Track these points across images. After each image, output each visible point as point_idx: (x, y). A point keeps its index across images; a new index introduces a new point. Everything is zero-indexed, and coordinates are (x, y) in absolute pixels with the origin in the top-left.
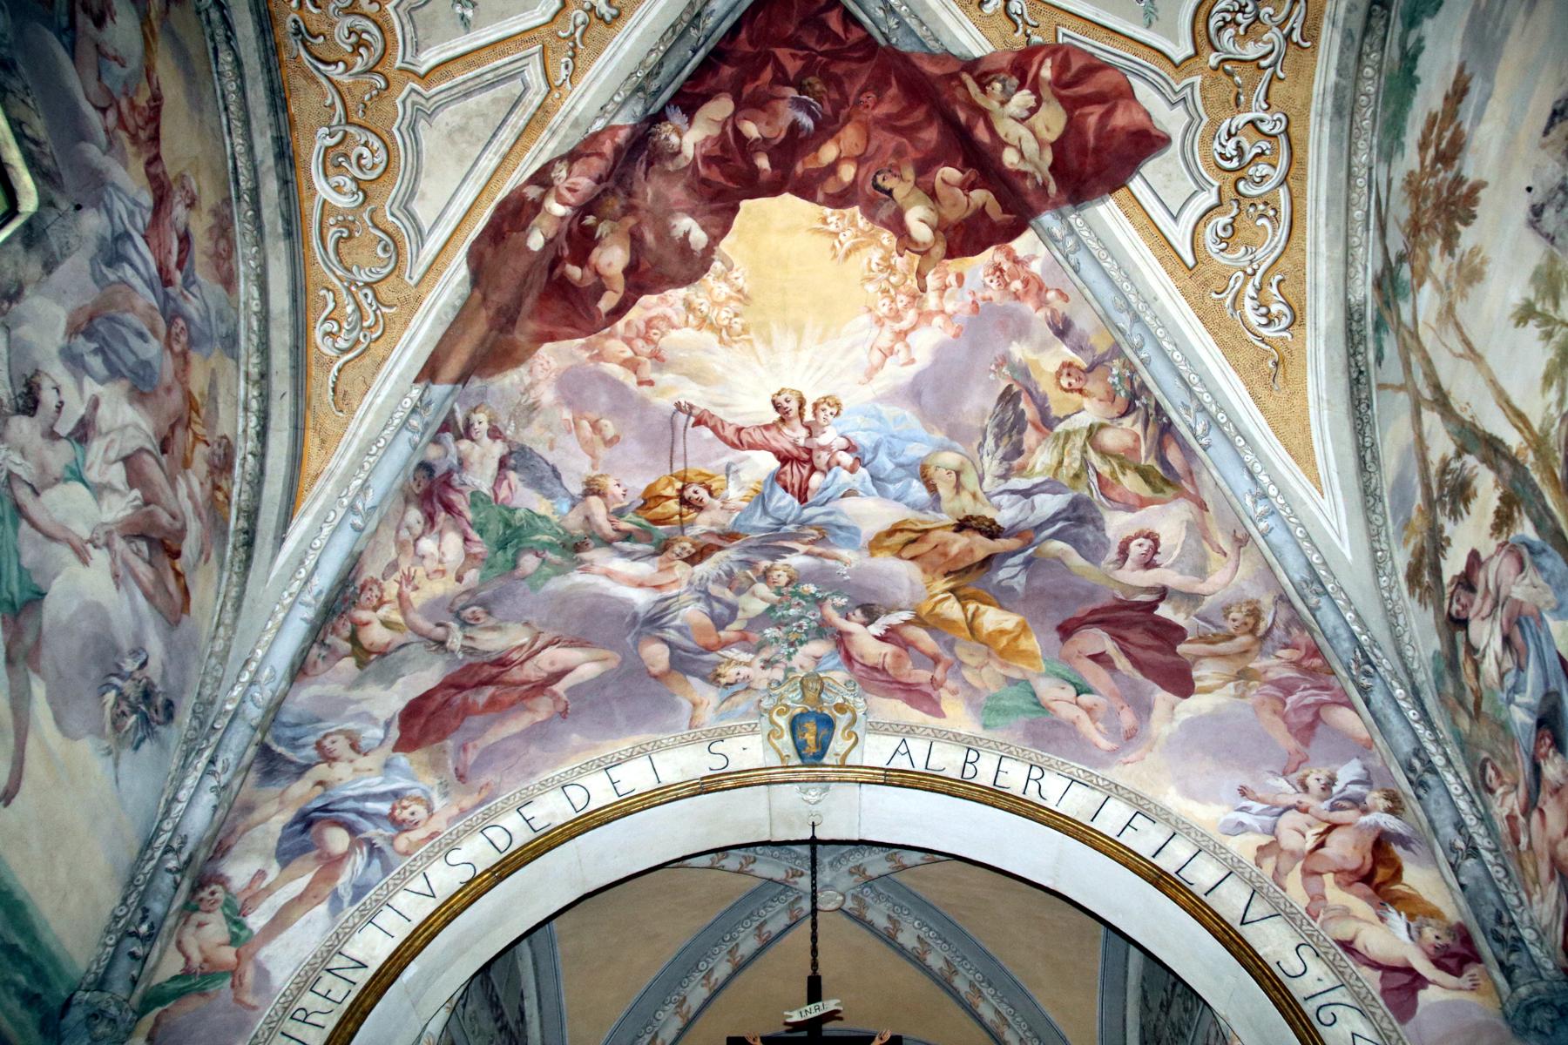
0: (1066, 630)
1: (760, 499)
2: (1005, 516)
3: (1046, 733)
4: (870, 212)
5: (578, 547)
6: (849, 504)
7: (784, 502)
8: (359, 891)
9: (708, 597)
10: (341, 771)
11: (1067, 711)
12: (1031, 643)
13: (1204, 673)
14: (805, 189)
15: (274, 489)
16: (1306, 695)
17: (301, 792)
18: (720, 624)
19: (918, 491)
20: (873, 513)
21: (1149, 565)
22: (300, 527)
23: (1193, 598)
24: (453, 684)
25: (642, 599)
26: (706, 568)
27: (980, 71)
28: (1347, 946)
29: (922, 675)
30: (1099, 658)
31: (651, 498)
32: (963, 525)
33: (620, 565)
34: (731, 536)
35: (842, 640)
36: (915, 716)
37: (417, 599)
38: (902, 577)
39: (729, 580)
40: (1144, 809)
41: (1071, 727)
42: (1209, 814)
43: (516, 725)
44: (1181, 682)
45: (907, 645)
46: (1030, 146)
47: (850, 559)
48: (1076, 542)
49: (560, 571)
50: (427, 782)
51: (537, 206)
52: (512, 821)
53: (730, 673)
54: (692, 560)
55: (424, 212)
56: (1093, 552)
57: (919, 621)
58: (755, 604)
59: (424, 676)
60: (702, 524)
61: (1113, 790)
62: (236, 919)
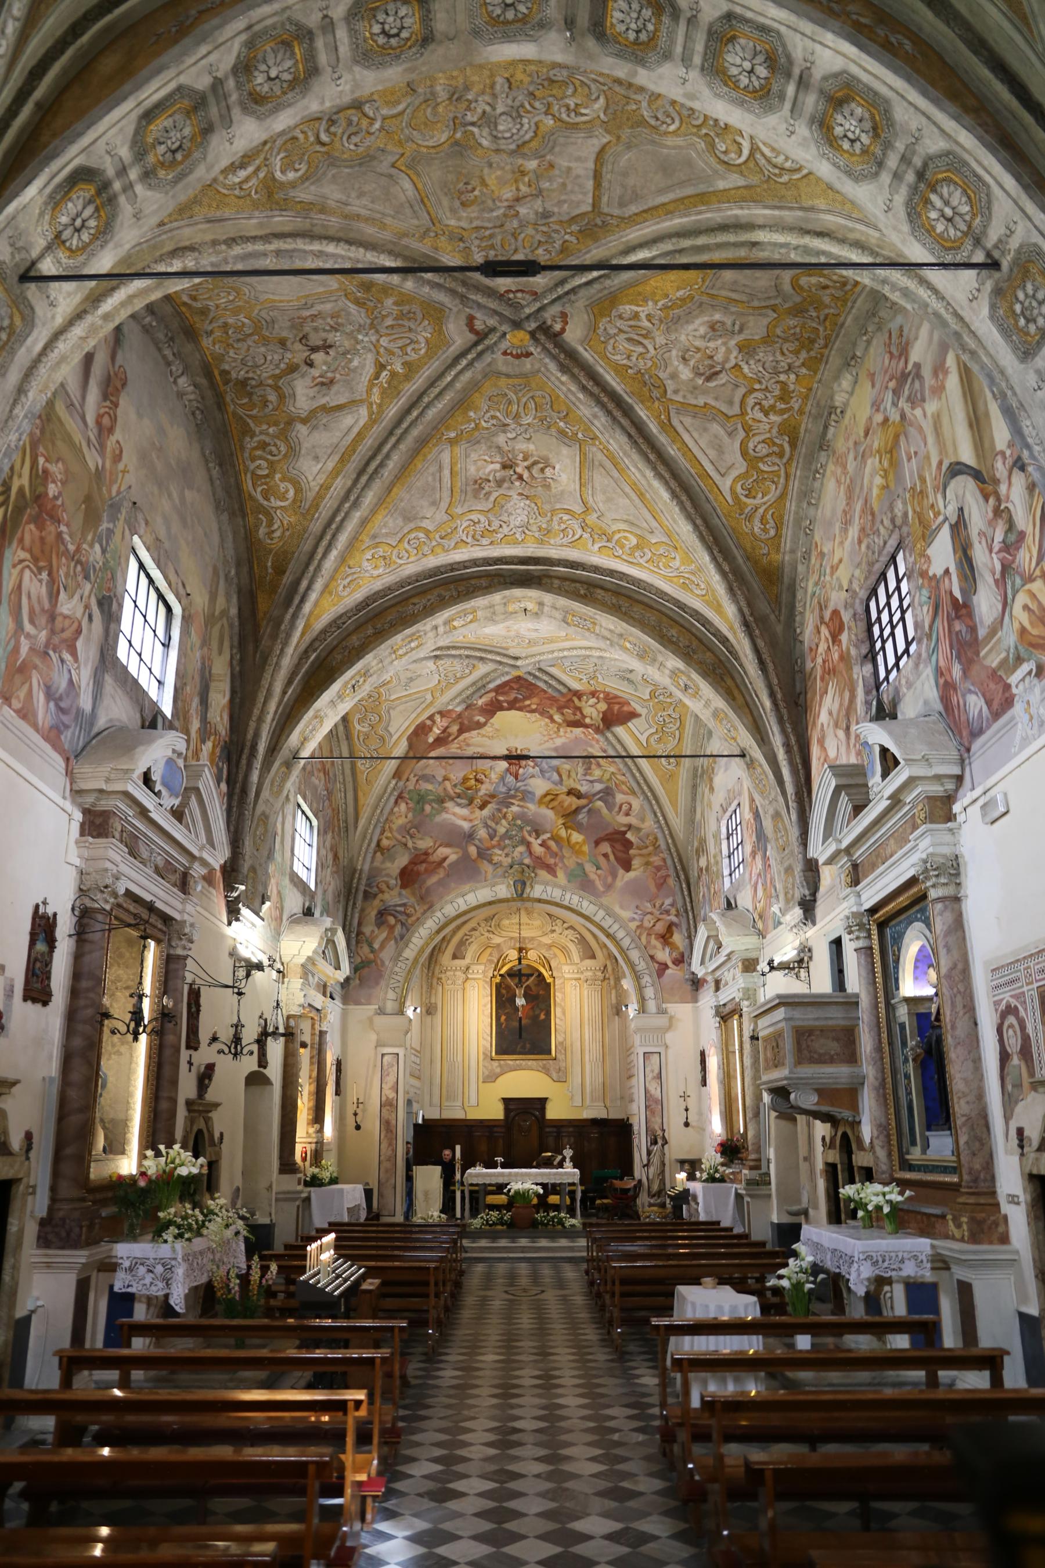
0: (597, 843)
1: (502, 778)
2: (583, 789)
3: (585, 885)
4: (542, 714)
5: (443, 801)
6: (532, 781)
7: (510, 779)
8: (402, 937)
9: (487, 826)
10: (386, 896)
11: (593, 876)
12: (586, 848)
13: (636, 863)
14: (520, 709)
15: (351, 810)
16: (663, 873)
17: (376, 903)
18: (492, 838)
19: (555, 776)
20: (539, 786)
21: (627, 814)
22: (362, 822)
23: (639, 830)
24: (414, 862)
25: (466, 825)
26: (486, 812)
27: (578, 694)
28: (652, 957)
29: (552, 861)
30: (605, 855)
31: (465, 779)
32: (570, 792)
33: (458, 810)
34: (493, 796)
35: (528, 845)
36: (549, 877)
37: (394, 827)
38: (548, 815)
39: (493, 817)
40: (609, 913)
41: (592, 882)
42: (626, 914)
43: (433, 880)
44: (627, 866)
45: (548, 848)
46: (595, 714)
47: (532, 807)
48: (605, 802)
49: (439, 812)
50: (412, 900)
51: (431, 729)
52: (439, 914)
53: (496, 859)
54: (482, 807)
55: (392, 730)
56: (610, 807)
57: (552, 838)
58: (502, 830)
59: (402, 860)
60: (484, 789)
61: (601, 906)
62: (370, 946)
